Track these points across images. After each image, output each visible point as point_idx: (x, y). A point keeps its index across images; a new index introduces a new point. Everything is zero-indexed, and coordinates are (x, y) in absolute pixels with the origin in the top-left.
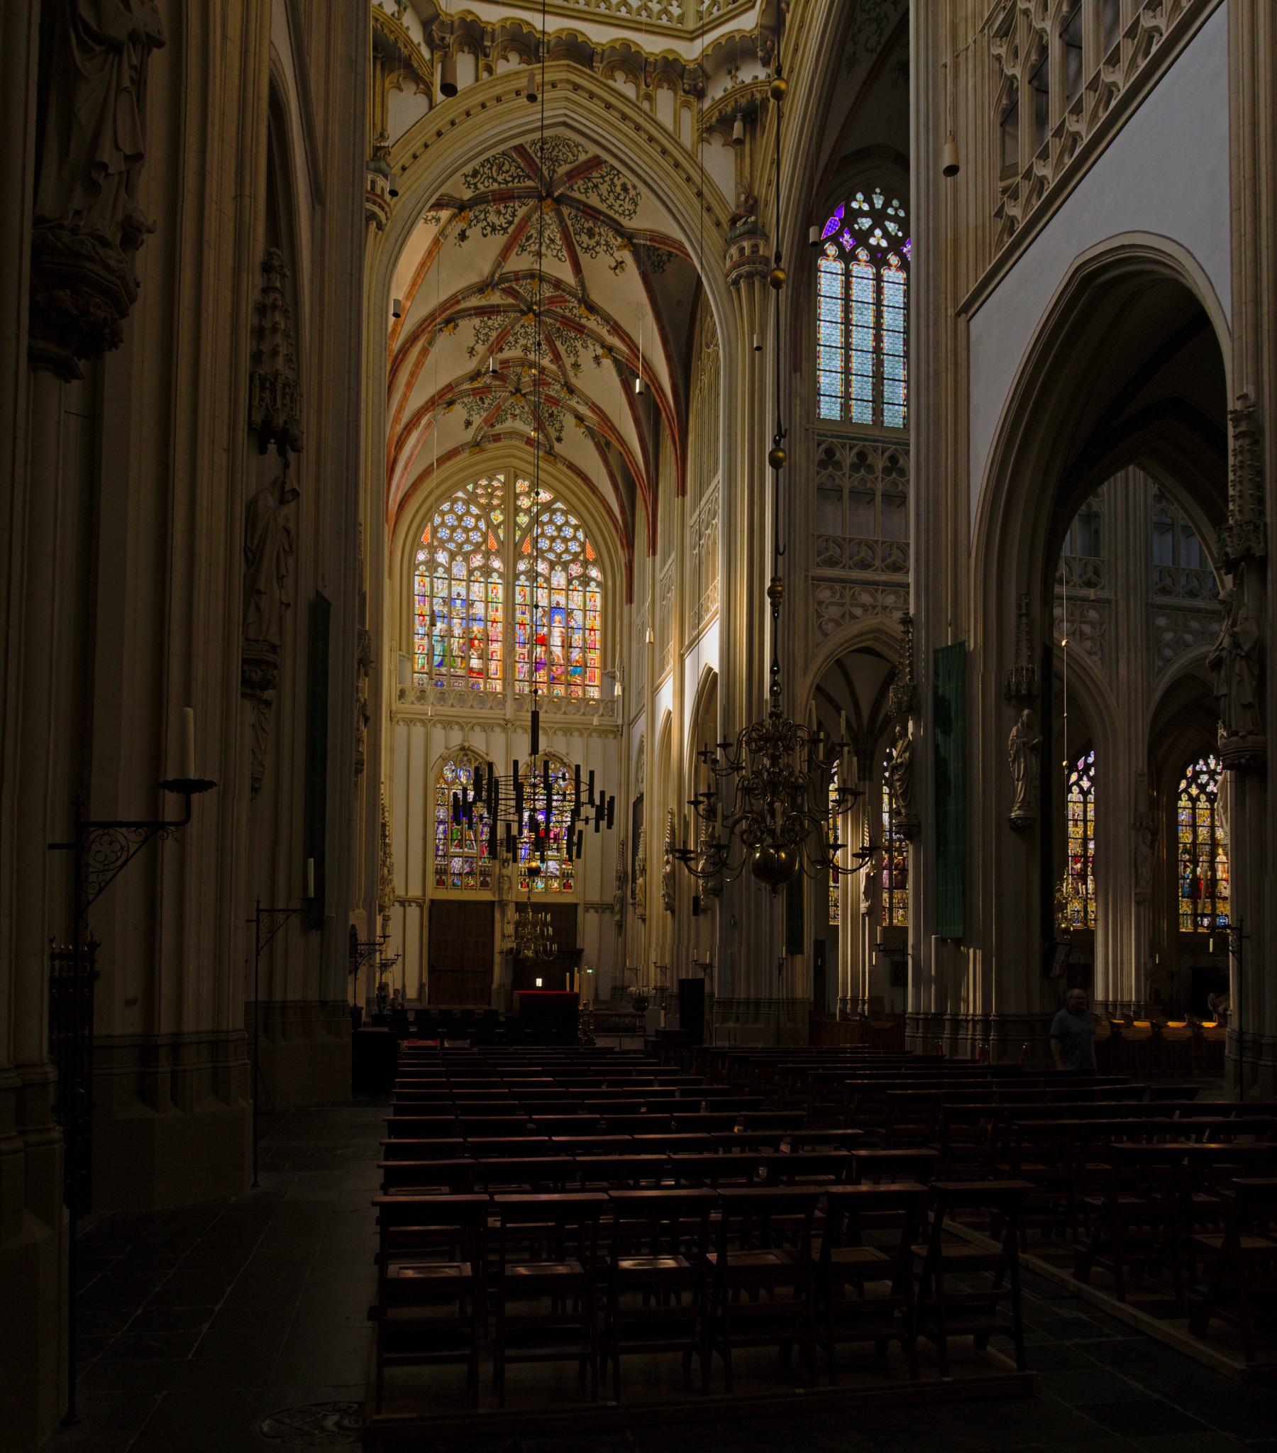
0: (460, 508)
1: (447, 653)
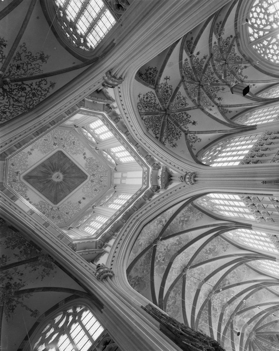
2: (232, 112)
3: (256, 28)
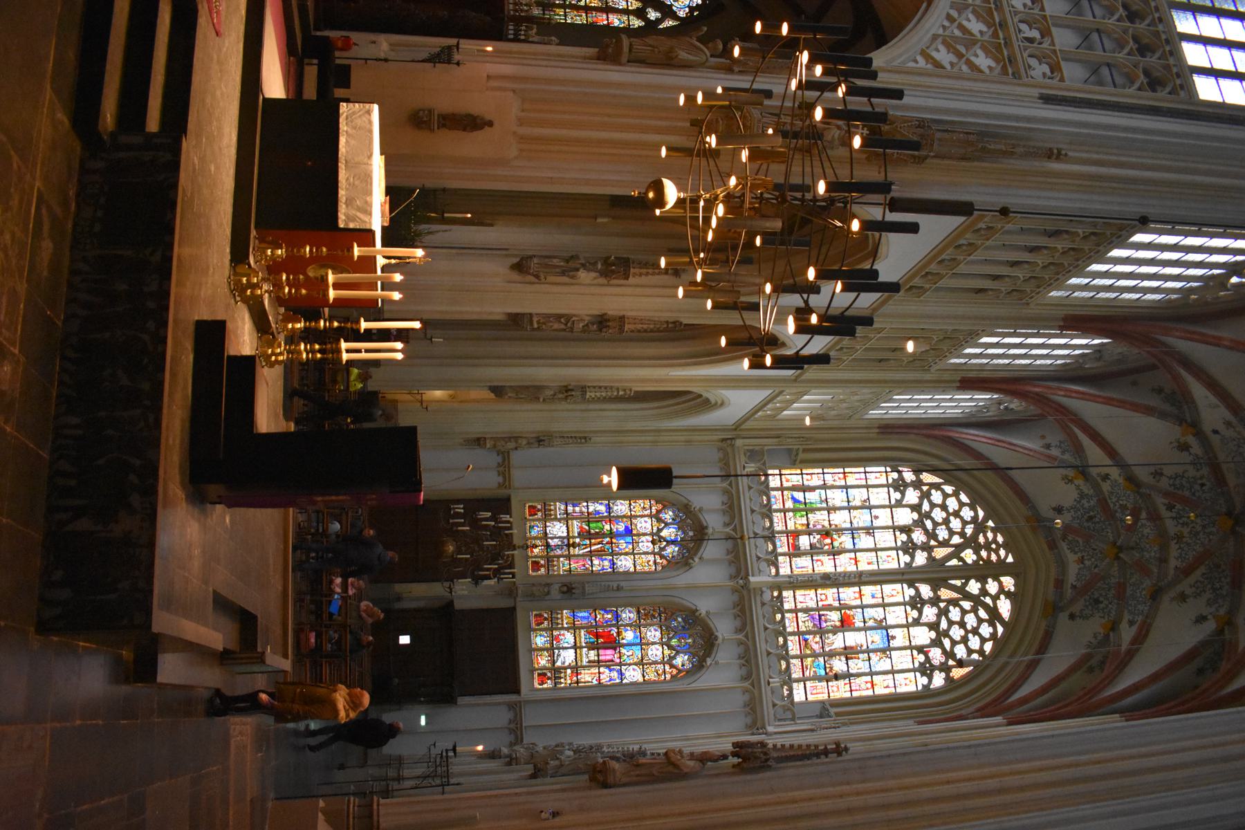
0: (967, 513)
1: (809, 509)
2: (1153, 390)
3: (986, 606)
